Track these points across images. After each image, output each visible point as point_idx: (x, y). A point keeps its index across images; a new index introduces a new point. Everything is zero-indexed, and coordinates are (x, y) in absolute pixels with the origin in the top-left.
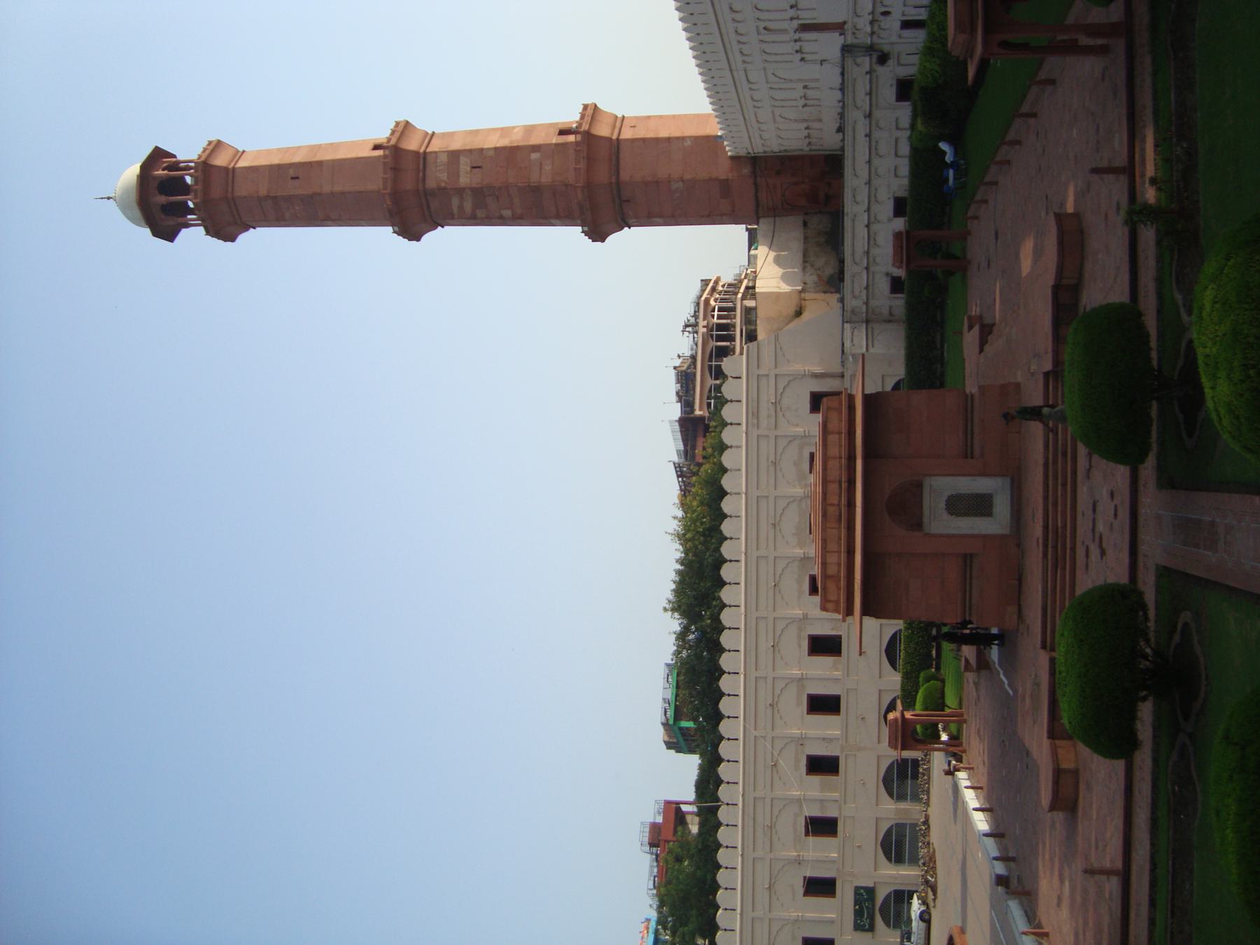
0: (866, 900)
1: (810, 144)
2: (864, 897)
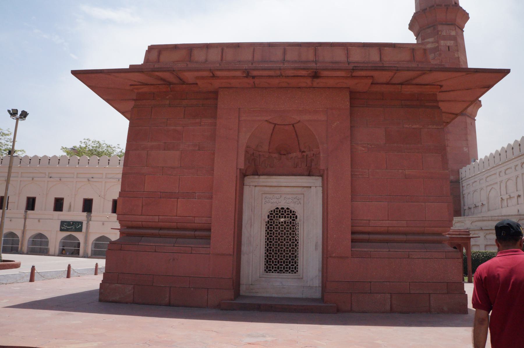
0: (75, 228)
1: (470, 208)
2: (76, 226)
